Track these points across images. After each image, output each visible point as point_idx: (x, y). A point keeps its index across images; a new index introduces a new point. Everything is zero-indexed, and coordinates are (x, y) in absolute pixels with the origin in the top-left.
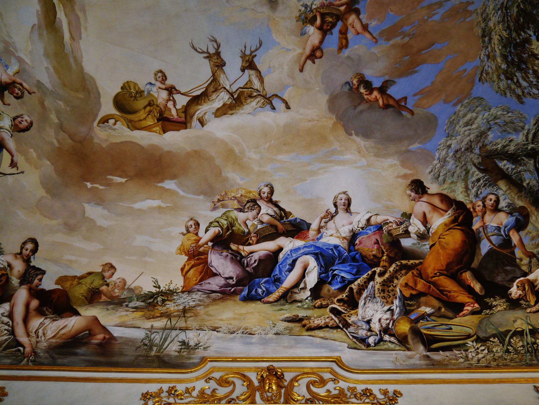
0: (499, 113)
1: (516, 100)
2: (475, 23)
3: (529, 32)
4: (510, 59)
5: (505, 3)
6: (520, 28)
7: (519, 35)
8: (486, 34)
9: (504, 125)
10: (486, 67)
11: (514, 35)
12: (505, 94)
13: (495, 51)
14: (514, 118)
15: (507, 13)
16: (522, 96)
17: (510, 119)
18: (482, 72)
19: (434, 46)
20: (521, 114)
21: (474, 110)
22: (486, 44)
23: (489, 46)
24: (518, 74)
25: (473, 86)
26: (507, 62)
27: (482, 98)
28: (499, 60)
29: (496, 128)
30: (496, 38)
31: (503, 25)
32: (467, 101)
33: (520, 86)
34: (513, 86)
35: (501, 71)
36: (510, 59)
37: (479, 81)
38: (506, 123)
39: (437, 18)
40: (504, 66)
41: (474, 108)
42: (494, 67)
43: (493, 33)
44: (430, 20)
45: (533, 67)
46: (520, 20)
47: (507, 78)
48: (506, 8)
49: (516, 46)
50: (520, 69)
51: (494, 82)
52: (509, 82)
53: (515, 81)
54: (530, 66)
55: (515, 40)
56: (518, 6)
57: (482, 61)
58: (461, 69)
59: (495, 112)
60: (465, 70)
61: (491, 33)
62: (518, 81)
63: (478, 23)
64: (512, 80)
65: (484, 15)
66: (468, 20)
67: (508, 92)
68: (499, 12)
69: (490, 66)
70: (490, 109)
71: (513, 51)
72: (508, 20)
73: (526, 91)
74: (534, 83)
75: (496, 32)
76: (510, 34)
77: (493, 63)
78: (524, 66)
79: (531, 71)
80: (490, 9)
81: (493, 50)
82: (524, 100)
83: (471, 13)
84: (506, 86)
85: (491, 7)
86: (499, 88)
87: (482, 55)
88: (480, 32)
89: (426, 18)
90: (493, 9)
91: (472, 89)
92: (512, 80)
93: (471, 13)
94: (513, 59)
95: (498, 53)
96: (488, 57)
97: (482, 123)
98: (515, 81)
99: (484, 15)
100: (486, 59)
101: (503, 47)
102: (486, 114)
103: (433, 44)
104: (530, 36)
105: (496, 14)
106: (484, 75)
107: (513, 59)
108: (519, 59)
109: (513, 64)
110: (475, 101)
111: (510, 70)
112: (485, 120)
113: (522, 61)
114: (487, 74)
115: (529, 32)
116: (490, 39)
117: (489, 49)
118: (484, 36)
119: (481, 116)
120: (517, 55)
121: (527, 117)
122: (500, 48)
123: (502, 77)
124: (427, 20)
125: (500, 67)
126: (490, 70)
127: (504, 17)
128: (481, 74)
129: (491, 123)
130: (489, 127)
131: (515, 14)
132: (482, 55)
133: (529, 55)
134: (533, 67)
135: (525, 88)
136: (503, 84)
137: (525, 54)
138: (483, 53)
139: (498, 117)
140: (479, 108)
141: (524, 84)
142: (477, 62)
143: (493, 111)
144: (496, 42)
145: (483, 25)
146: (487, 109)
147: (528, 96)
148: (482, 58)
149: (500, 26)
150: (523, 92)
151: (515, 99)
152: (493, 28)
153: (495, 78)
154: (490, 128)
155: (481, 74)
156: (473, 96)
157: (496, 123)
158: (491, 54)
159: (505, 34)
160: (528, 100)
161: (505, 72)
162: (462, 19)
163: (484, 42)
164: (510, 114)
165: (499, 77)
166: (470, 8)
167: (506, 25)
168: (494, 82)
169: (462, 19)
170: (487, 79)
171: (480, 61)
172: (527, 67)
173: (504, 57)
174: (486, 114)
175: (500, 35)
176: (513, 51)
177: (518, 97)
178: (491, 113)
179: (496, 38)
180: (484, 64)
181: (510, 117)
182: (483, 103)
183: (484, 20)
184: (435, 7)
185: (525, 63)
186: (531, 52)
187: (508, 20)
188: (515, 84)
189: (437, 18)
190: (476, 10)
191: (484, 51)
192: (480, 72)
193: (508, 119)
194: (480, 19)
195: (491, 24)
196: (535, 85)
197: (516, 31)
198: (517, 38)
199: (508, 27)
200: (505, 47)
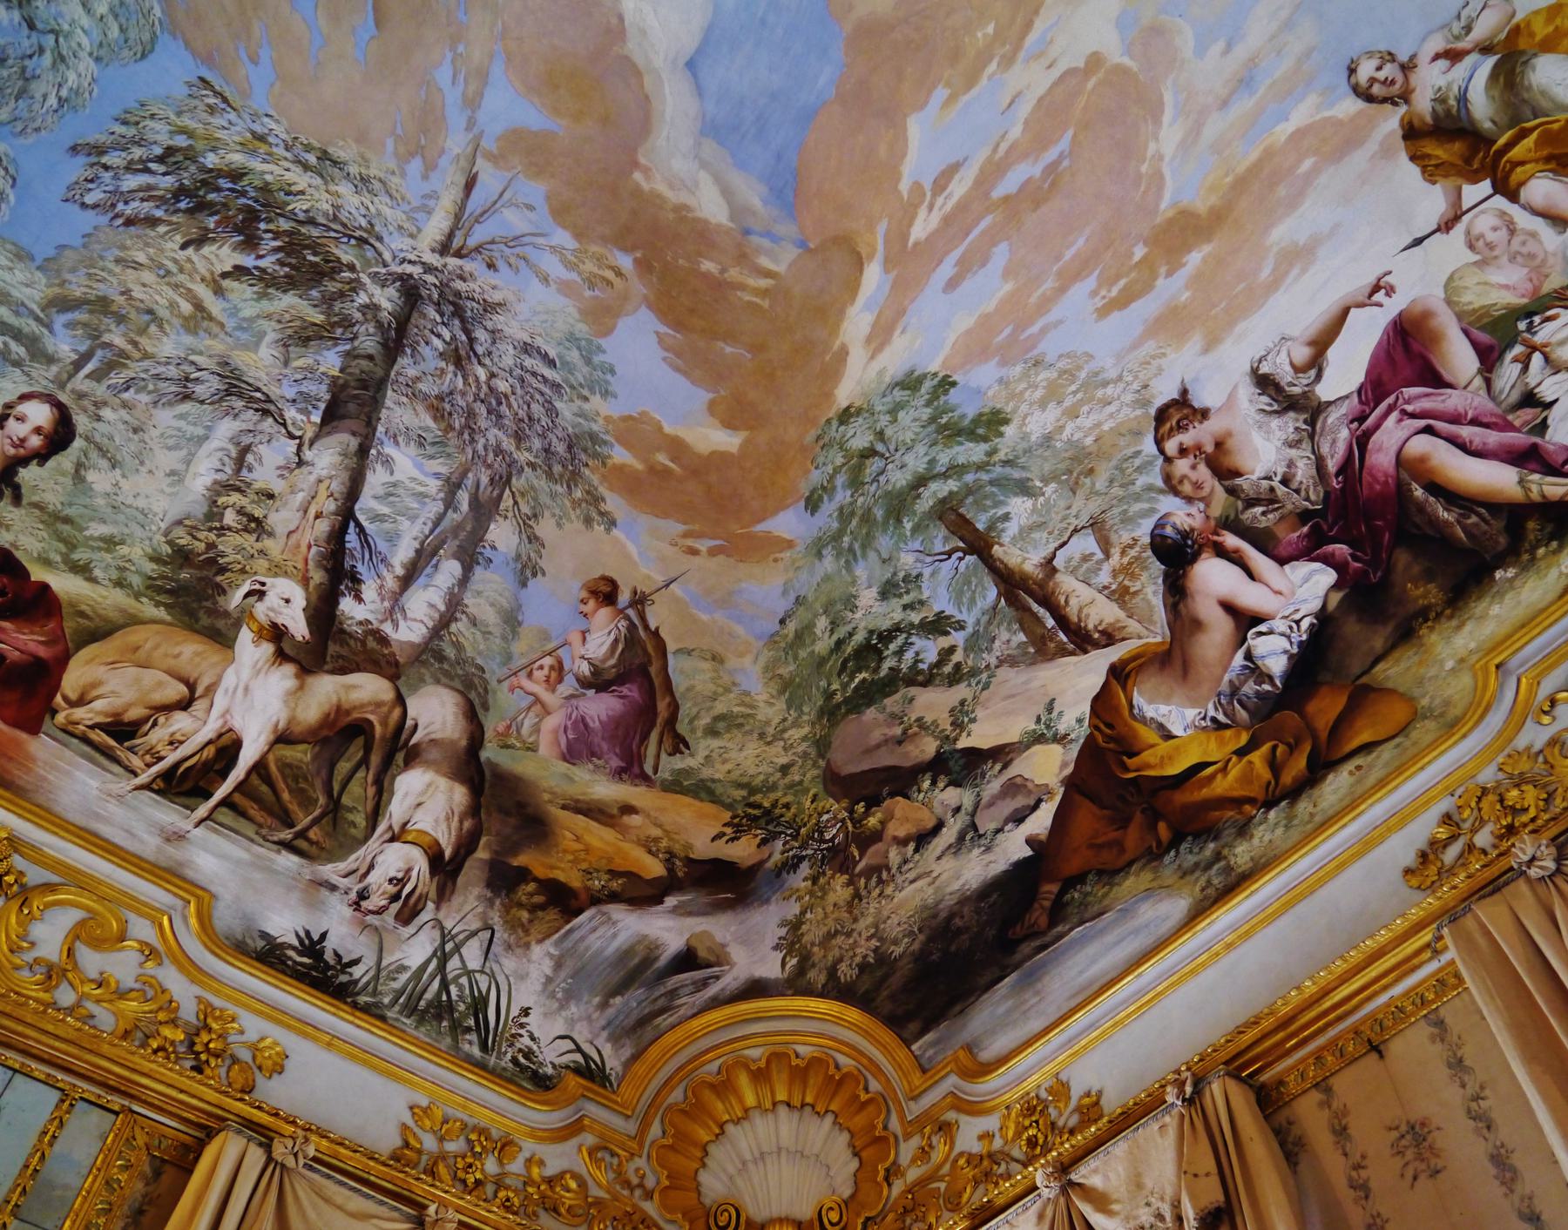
0: (72, 77)
1: (91, 140)
2: (369, 155)
3: (273, 258)
4: (224, 183)
5: (377, 245)
6: (293, 245)
7: (277, 235)
8: (326, 163)
9: (24, 69)
10: (232, 116)
11: (284, 225)
12: (125, 123)
13: (265, 161)
14: (36, 107)
15: (350, 237)
16: (95, 160)
17: (38, 96)
18: (225, 100)
19: (371, 23)
20: (37, 130)
21: (116, 16)
22: (298, 149)
23: (288, 155)
24: (169, 182)
25: (194, 54)
26: (219, 173)
27: (144, 56)
28: (237, 159)
29: (26, 43)
30: (300, 179)
31: (326, 214)
32: (157, 11)
33: (130, 168)
34: (137, 153)
35: (200, 145)
36: (224, 183)
37: (202, 80)
38: (27, 77)
39: (443, 76)
40: (211, 160)
41: (123, 21)
42: (220, 134)
43: (318, 181)
44: (449, 55)
45: (170, 223)
46: (315, 254)
47: (170, 151)
48: (362, 241)
49: (252, 216)
50: (180, 192)
51: (179, 114)
52: (158, 151)
53: (153, 166)
54: (174, 219)
55: (269, 220)
56: (352, 268)
57: (255, 116)
58: (265, 55)
59: (81, 68)
60: (255, 61)
61: (322, 176)
62: (147, 171)
63: (366, 162)
64: (160, 159)
65: (377, 185)
66: (390, 143)
67: (131, 132)
68: (364, 223)
69: (230, 129)
70: (98, 60)
71: (243, 201)
72: (330, 229)
73: (107, 176)
74: (120, 206)
75: (317, 188)
76: (292, 216)
77: (237, 139)
78: (182, 205)
79: (159, 213)
80: (382, 205)
81: (270, 158)
82: (82, 160)
83: (403, 159)
84: (150, 136)
85: (387, 211)
86: (152, 116)
87: (274, 126)
88: (336, 152)
89: (461, 49)
90: (379, 214)
91: (187, 44)
92: (160, 159)
93: (403, 159)
94: (218, 190)
95: (256, 165)
96: (261, 138)
97: (60, 14)
98: (153, 166)
99: (377, 185)
100: (258, 128)
101: (267, 184)
102: (85, 42)
103: (378, 23)
104: (260, 257)
105: (363, 211)
106: (212, 101)
107: (218, 190)
108: (212, 204)
109: (204, 183)
110: (146, 37)
111: (193, 169)
112: (66, 27)
113: (202, 207)
114: (211, 109)
115: (273, 258)
116: (306, 167)
117: (280, 151)
118: (324, 156)
119: (85, 21)
120: (225, 205)
121: (21, 141)
122: (269, 178)
123: (181, 141)
124: (453, 49)
125: (214, 150)
126: (218, 121)
127: (344, 225)
128: (217, 94)
129: (51, 39)
130: (39, 25)
131: (335, 251)
132: (274, 126)
133: (207, 230)
134: (170, 223)
135: (116, 177)
136: (161, 135)
137: (218, 223)
138: (279, 130)
139: (62, 67)
140: (114, 32)
141: (131, 182)
142: (259, 102)
143: (86, 65)
144: (289, 176)
145: (353, 170)
146: (102, 52)
147: (89, 174)
148: (266, 120)
149: (326, 207)
150: (106, 167)
151: (103, 138)
152: (333, 188)
153: (187, 121)
154: (31, 26)
155: (217, 94)
156: (164, 39)
157: (41, 50)
158: (263, 148)
159: (298, 206)
160: (77, 168)
161: (190, 155)
162: (399, 131)
163: (308, 148)
164: (52, 101)
165: (190, 134)
166: (415, 166)
167: (321, 220)
168: (179, 114)
169: (399, 131)
170: (196, 102)
171: (261, 112)
172: (177, 211)
173: (236, 175)
174: (85, 42)
175: (302, 193)
176: (243, 201)
177: (100, 150)
178: (83, 55)
179: (300, 179)
180: (246, 116)
181: (45, 97)
182: (126, 53)
183: (365, 180)
184: (472, 88)
185: (189, 211)
186: (214, 239)
187: (330, 229)
188: (141, 161)
189: (443, 76)
190: (403, 175)
191: (284, 136)
192: (227, 94)
193: (38, 88)
194: (373, 172)
195: (345, 189)
196: (113, 206)
197: (289, 233)
198: (271, 226)
199: (312, 222)
200: (265, 188)
